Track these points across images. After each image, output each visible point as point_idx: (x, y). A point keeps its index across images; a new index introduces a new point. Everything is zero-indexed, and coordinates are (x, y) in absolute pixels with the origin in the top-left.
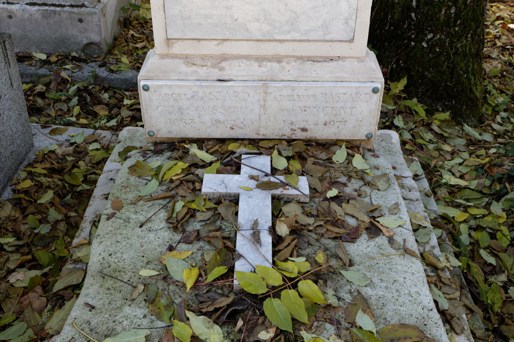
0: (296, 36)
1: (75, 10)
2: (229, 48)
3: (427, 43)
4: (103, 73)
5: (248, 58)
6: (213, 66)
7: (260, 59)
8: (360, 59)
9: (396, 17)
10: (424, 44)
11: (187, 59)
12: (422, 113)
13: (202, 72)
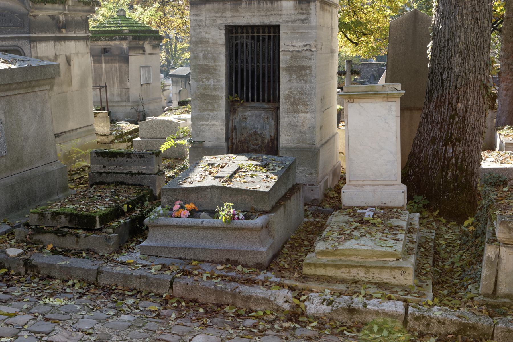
0: (382, 179)
1: (310, 186)
2: (365, 182)
3: (447, 196)
4: (319, 208)
5: (370, 185)
6: (361, 187)
7: (373, 185)
8: (399, 185)
9: (436, 188)
10: (445, 197)
11: (354, 185)
12: (444, 221)
13: (358, 188)
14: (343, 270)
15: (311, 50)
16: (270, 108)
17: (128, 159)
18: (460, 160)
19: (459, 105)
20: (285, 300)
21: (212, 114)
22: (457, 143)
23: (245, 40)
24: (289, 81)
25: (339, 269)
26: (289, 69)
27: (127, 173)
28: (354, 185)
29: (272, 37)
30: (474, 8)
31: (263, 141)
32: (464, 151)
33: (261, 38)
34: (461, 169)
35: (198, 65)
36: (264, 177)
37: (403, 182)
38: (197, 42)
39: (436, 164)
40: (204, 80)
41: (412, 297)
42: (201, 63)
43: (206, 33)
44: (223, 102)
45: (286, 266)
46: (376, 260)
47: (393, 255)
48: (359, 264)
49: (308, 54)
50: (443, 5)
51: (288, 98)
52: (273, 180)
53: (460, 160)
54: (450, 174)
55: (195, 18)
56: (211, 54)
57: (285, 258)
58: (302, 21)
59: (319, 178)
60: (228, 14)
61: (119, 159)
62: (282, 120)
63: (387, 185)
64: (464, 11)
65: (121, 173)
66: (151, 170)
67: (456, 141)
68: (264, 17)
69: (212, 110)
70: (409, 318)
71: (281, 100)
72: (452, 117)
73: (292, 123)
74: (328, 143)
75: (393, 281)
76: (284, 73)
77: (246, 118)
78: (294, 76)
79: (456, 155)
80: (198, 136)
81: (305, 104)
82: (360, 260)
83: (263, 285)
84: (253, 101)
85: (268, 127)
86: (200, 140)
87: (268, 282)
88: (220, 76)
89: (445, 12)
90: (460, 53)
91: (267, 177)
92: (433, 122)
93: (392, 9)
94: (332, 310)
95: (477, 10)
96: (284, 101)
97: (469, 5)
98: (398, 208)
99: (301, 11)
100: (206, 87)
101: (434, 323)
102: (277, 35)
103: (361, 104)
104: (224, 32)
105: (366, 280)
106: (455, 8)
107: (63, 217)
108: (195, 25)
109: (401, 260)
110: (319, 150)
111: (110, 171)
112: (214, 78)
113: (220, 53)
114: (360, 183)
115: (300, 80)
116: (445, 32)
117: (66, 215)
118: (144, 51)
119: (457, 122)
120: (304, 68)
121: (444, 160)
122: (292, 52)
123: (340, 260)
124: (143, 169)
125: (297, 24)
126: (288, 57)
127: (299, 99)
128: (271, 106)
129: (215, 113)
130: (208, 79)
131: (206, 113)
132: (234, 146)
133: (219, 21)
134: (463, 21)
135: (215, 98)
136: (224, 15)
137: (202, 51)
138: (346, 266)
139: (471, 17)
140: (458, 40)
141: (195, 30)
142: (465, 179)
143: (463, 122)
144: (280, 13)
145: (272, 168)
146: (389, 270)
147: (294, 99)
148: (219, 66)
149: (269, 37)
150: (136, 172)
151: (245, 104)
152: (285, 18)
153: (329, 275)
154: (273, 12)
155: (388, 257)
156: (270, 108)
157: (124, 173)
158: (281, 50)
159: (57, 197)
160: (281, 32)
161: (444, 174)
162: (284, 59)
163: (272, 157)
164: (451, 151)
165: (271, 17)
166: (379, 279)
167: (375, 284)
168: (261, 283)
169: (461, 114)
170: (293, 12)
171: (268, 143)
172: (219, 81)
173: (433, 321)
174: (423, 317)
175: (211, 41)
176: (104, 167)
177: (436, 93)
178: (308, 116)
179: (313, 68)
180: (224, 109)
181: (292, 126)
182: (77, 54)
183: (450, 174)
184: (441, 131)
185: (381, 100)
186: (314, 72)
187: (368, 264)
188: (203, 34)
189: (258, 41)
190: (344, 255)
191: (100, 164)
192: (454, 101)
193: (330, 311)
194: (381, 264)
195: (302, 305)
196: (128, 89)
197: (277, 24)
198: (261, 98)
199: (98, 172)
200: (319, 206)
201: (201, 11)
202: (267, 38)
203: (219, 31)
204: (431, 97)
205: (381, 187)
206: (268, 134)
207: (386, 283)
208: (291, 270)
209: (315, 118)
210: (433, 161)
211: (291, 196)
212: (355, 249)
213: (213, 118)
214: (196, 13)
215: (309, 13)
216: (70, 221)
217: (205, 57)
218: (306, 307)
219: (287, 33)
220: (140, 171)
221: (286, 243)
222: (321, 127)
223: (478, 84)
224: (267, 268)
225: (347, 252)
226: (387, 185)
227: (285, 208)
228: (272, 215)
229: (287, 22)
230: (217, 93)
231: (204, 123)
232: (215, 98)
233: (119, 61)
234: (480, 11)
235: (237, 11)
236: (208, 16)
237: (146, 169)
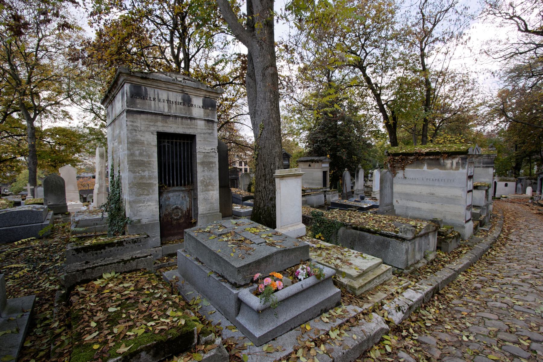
17: (119, 247)
21: (148, 197)
23: (166, 144)
24: (203, 171)
26: (203, 163)
27: (119, 262)
33: (182, 144)
35: (135, 160)
38: (133, 143)
40: (140, 172)
42: (138, 158)
43: (141, 136)
51: (202, 182)
55: (131, 123)
58: (210, 134)
60: (159, 124)
61: (108, 249)
65: (111, 264)
66: (146, 253)
69: (148, 195)
78: (206, 168)
80: (135, 216)
84: (173, 185)
85: (185, 202)
86: (138, 218)
88: (153, 169)
94: (403, 313)
100: (142, 177)
107: (143, 354)
108: (132, 130)
111: (96, 265)
112: (149, 170)
113: (154, 152)
117: (148, 349)
124: (137, 253)
126: (202, 156)
127: (209, 182)
128: (187, 189)
129: (150, 196)
130: (144, 171)
131: (142, 197)
133: (152, 129)
135: (150, 185)
136: (156, 124)
137: (138, 150)
141: (131, 133)
148: (153, 161)
150: (130, 258)
152: (199, 131)
154: (192, 127)
157: (115, 263)
162: (199, 157)
165: (190, 129)
170: (204, 128)
172: (153, 172)
175: (146, 142)
176: (87, 263)
181: (205, 200)
188: (139, 137)
193: (403, 315)
198: (179, 183)
199: (78, 271)
201: (137, 119)
202: (182, 144)
203: (152, 135)
213: (148, 201)
214: (132, 120)
215: (213, 130)
217: (141, 154)
220: (134, 257)
229: (201, 133)
230: (152, 181)
231: (141, 205)
232: (150, 185)
235: (166, 122)
237: (141, 253)
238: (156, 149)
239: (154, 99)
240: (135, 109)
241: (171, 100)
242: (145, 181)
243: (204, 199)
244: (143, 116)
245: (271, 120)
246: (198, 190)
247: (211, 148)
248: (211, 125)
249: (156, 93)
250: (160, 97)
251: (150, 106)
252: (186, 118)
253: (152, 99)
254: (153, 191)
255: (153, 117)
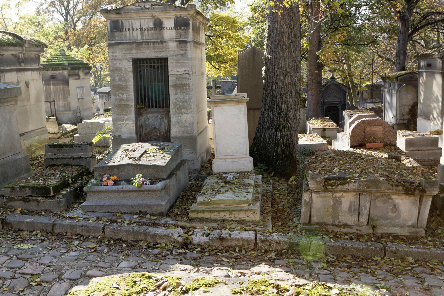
2: (227, 157)
4: (199, 175)
7: (232, 158)
11: (220, 159)
12: (277, 179)
14: (215, 213)
15: (189, 74)
16: (164, 112)
18: (285, 140)
19: (283, 106)
20: (179, 235)
21: (126, 117)
22: (283, 130)
24: (176, 94)
25: (213, 213)
26: (175, 86)
27: (71, 158)
28: (220, 159)
29: (163, 66)
30: (290, 45)
31: (160, 133)
32: (287, 134)
33: (156, 67)
34: (286, 146)
35: (116, 85)
36: (162, 156)
37: (250, 155)
38: (114, 70)
39: (270, 143)
40: (120, 95)
41: (259, 228)
42: (117, 83)
43: (120, 64)
44: (133, 109)
45: (179, 213)
46: (236, 206)
47: (246, 202)
48: (225, 209)
49: (187, 76)
50: (271, 44)
51: (175, 105)
52: (168, 158)
53: (285, 140)
54: (280, 149)
55: (112, 54)
56: (124, 77)
57: (178, 208)
58: (182, 55)
59: (198, 156)
60: (134, 51)
61: (65, 148)
62: (172, 119)
63: (241, 158)
64: (284, 47)
65: (67, 158)
66: (87, 155)
67: (282, 128)
68: (158, 53)
69: (126, 115)
70: (258, 241)
71: (171, 106)
72: (279, 114)
73: (179, 121)
74: (203, 133)
75: (247, 219)
76: (172, 89)
77: (148, 119)
78: (179, 91)
79: (283, 137)
80: (117, 132)
81: (186, 108)
82: (225, 207)
83: (164, 226)
84: (152, 107)
85: (163, 124)
86: (119, 134)
87: (167, 224)
88: (130, 92)
89: (272, 48)
90: (283, 73)
91: (164, 156)
92: (268, 117)
93: (239, 46)
94: (209, 239)
95: (292, 46)
96: (173, 107)
97: (286, 43)
98: (248, 172)
99: (181, 49)
100: (122, 100)
101: (273, 244)
102: (166, 64)
103: (222, 107)
104: (132, 63)
105: (230, 219)
106: (278, 45)
107: (27, 189)
108: (112, 59)
109: (251, 205)
110: (197, 137)
112: (126, 94)
114: (224, 157)
115: (183, 93)
116: (272, 60)
117: (30, 188)
118: (79, 77)
119: (282, 117)
120: (185, 85)
121: (275, 141)
122: (177, 75)
123: (213, 207)
124: (81, 154)
125: (179, 57)
126: (174, 78)
127: (183, 105)
128: (164, 110)
129: (128, 116)
130: (122, 94)
131: (122, 116)
132: (142, 137)
133: (128, 56)
134: (283, 53)
135: (127, 106)
137: (118, 76)
138: (217, 211)
139: (288, 51)
140: (281, 65)
141: (112, 62)
142: (289, 152)
143: (286, 116)
144: (168, 50)
145: (167, 150)
146: (244, 212)
147: (179, 105)
148: (129, 85)
149: (161, 66)
150: (77, 157)
151: (148, 109)
152: (171, 53)
153: (207, 217)
154: (163, 50)
155: (243, 204)
156: (164, 112)
158: (169, 74)
159: (23, 176)
160: (169, 62)
161: (276, 149)
162: (172, 80)
163: (167, 143)
164: (280, 134)
166: (238, 218)
167: (236, 221)
168: (162, 225)
169: (285, 111)
170: (176, 49)
171: (164, 134)
172: (130, 95)
173: (273, 242)
174: (267, 240)
175: (123, 69)
176: (55, 154)
177: (269, 98)
178: (189, 116)
179: (191, 85)
180: (134, 113)
181: (179, 122)
182: (33, 80)
183: (280, 149)
184: (273, 123)
185: (234, 104)
186: (191, 88)
187: (230, 209)
188: (118, 64)
189: (154, 68)
190: (215, 204)
191: (52, 153)
192: (280, 103)
193: (208, 240)
194: (239, 209)
195: (190, 238)
196: (69, 103)
197: (166, 57)
198: (158, 105)
199: (50, 158)
200: (199, 174)
202: (160, 66)
203: (128, 63)
204: (266, 101)
205: (237, 160)
206: (163, 128)
207: (243, 220)
208: (182, 215)
209: (193, 117)
210: (268, 142)
211: (180, 168)
212: (222, 200)
213: (127, 120)
214: (112, 51)
215: (186, 50)
216: (33, 192)
217: (120, 80)
218: (192, 239)
219: (173, 63)
220: (79, 156)
221: (178, 198)
222: (197, 123)
223: (294, 92)
224: (166, 215)
225: (217, 202)
226: (241, 158)
227: (176, 176)
228: (168, 181)
229: (173, 56)
230: (129, 103)
231: (121, 123)
232: (127, 106)
233: (63, 84)
234: (293, 47)
235: (140, 49)
236: (120, 53)
237: (83, 155)
238: (131, 75)
239: (129, 29)
240: (113, 42)
241: (144, 27)
242: (123, 103)
243: (177, 121)
244: (120, 46)
245: (276, 25)
246: (171, 112)
247: (184, 69)
248: (183, 45)
249: (130, 23)
250: (134, 26)
251: (126, 36)
252: (157, 42)
253: (127, 30)
254: (130, 111)
255: (129, 46)
